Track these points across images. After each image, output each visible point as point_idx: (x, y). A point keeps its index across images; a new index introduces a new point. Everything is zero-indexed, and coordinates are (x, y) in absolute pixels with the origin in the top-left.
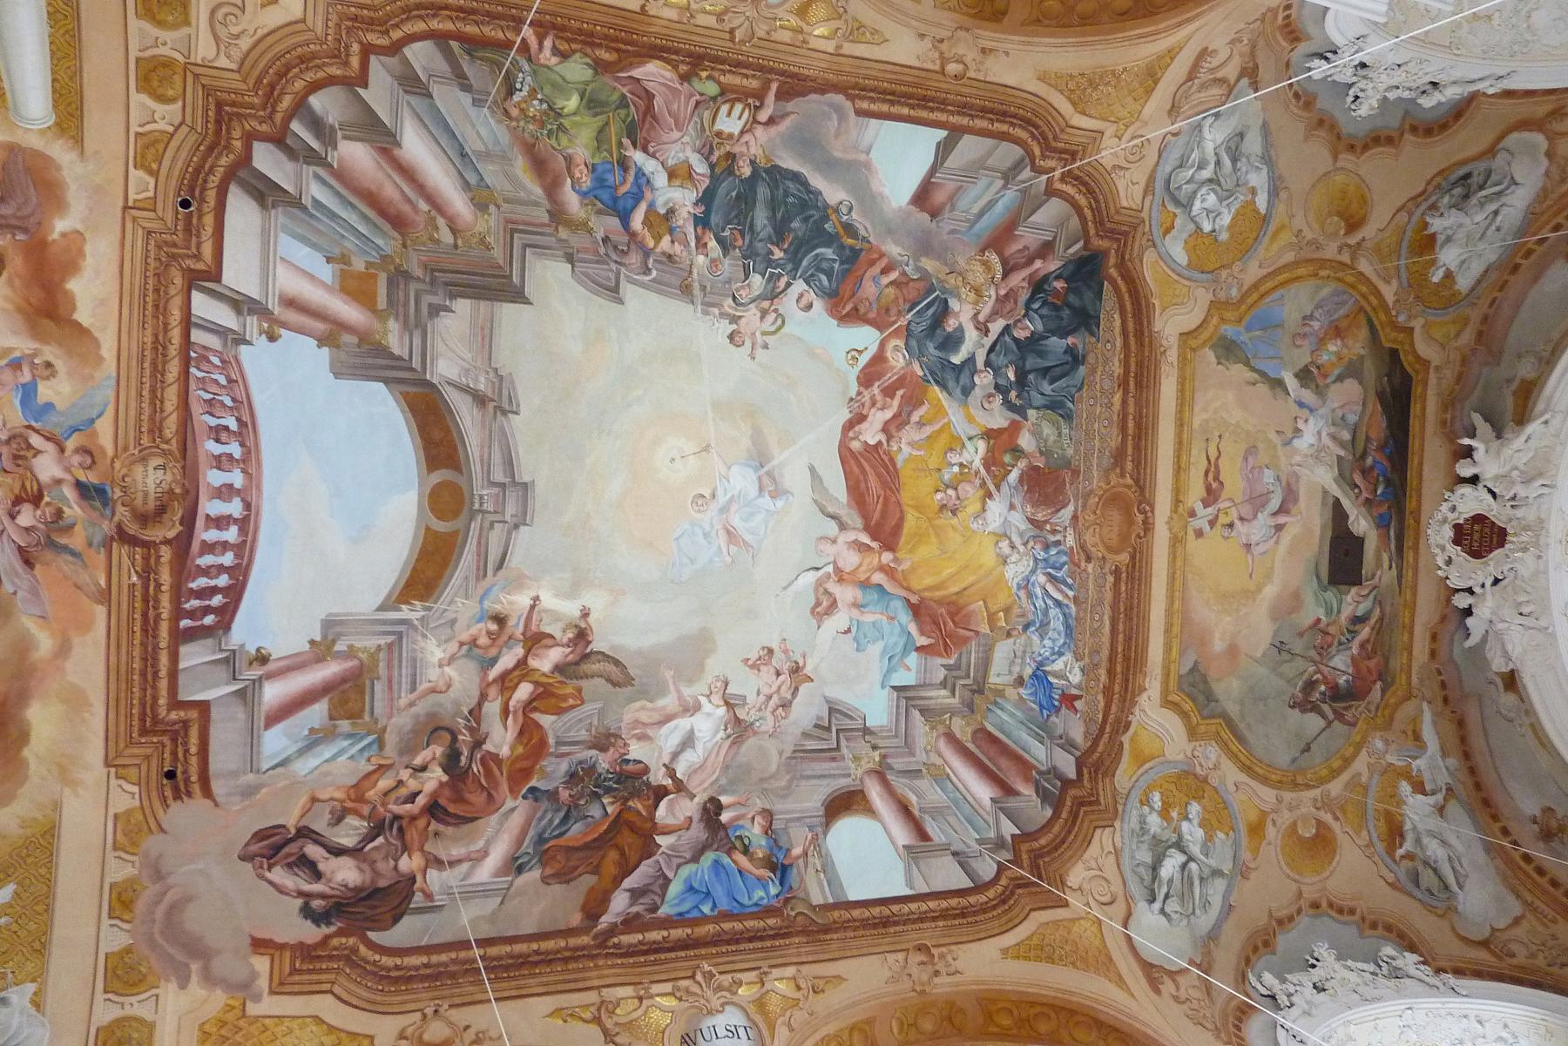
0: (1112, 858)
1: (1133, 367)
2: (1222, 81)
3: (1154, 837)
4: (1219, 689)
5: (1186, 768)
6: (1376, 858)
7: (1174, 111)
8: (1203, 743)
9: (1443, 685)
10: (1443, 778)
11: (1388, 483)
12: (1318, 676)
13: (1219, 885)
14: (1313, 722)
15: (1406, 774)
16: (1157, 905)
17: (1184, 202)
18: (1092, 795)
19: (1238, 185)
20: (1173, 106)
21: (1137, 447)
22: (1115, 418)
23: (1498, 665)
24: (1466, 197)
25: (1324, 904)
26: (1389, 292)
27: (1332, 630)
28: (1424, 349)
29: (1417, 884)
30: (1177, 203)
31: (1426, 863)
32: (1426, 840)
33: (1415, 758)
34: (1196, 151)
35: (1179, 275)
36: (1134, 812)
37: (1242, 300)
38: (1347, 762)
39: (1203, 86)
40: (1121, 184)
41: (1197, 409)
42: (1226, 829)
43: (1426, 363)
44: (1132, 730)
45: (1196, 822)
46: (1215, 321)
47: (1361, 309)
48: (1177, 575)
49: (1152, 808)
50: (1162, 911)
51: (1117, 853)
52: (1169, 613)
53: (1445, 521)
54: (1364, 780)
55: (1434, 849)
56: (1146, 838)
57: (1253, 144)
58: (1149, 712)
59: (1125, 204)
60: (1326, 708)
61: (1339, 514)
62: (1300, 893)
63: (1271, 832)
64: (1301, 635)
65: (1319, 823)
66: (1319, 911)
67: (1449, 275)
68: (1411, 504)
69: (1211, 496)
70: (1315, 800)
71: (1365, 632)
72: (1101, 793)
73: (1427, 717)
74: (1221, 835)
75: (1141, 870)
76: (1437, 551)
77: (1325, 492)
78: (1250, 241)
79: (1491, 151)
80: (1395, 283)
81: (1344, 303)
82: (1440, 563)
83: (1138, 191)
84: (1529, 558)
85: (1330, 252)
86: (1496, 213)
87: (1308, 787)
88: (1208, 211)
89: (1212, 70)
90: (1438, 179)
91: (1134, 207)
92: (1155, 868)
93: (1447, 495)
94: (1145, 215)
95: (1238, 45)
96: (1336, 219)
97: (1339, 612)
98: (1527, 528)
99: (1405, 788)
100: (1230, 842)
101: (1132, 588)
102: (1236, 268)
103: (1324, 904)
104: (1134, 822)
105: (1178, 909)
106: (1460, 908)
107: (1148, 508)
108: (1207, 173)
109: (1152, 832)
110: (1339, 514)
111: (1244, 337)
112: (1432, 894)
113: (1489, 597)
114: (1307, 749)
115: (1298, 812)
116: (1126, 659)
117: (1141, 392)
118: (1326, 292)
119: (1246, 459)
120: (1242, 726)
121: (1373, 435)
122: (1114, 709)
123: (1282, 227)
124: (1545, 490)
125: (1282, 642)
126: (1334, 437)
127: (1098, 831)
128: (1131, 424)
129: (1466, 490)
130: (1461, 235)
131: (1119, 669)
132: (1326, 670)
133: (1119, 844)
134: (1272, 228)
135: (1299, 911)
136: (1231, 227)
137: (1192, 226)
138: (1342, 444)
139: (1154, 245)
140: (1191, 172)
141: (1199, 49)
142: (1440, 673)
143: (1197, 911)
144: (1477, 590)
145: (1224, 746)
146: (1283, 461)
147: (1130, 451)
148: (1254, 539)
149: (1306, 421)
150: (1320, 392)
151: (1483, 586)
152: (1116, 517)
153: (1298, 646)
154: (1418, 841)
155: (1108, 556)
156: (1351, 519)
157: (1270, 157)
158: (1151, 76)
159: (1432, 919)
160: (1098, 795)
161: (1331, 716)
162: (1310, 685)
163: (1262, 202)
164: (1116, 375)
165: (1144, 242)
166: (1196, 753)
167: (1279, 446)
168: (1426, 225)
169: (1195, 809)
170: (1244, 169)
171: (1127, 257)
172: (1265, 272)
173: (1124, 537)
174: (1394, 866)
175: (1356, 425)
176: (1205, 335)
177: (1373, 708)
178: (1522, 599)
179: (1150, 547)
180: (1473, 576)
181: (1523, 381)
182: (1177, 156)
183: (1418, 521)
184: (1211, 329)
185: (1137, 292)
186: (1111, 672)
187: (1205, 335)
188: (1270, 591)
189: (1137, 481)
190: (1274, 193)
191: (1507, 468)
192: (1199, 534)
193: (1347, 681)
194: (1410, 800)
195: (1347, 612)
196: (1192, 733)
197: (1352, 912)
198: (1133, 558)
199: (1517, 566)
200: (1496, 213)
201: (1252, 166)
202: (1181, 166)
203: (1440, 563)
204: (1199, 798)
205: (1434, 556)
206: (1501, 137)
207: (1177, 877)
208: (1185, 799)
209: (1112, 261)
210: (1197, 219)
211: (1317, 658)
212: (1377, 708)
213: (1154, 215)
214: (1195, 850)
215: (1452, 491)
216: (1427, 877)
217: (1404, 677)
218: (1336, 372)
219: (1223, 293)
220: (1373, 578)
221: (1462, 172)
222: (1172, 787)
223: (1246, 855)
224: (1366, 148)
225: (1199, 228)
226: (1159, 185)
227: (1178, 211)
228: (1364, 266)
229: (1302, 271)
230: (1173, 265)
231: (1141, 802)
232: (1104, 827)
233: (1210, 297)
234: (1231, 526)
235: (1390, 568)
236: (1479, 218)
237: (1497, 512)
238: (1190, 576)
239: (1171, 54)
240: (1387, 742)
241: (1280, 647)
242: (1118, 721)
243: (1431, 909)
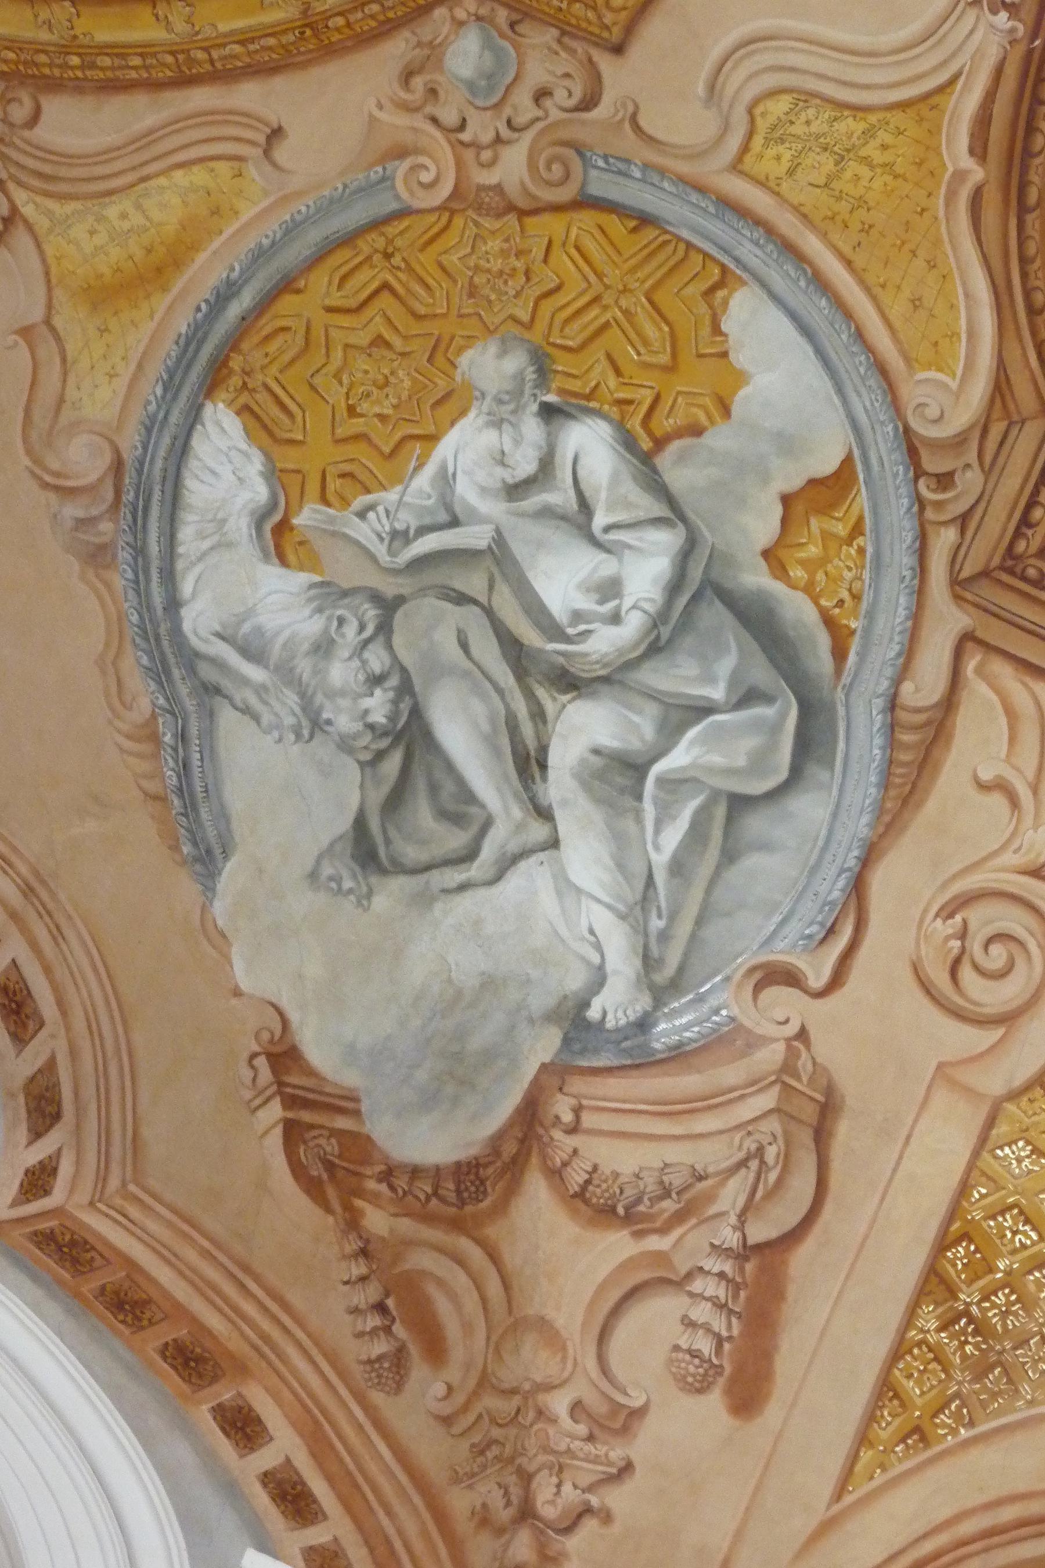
20: (822, 1136)
34: (661, 859)
35: (791, 250)
141: (773, 1413)
157: (160, 674)
165: (970, 481)
182: (751, 861)
201: (286, 673)
210: (649, 506)
219: (537, 74)
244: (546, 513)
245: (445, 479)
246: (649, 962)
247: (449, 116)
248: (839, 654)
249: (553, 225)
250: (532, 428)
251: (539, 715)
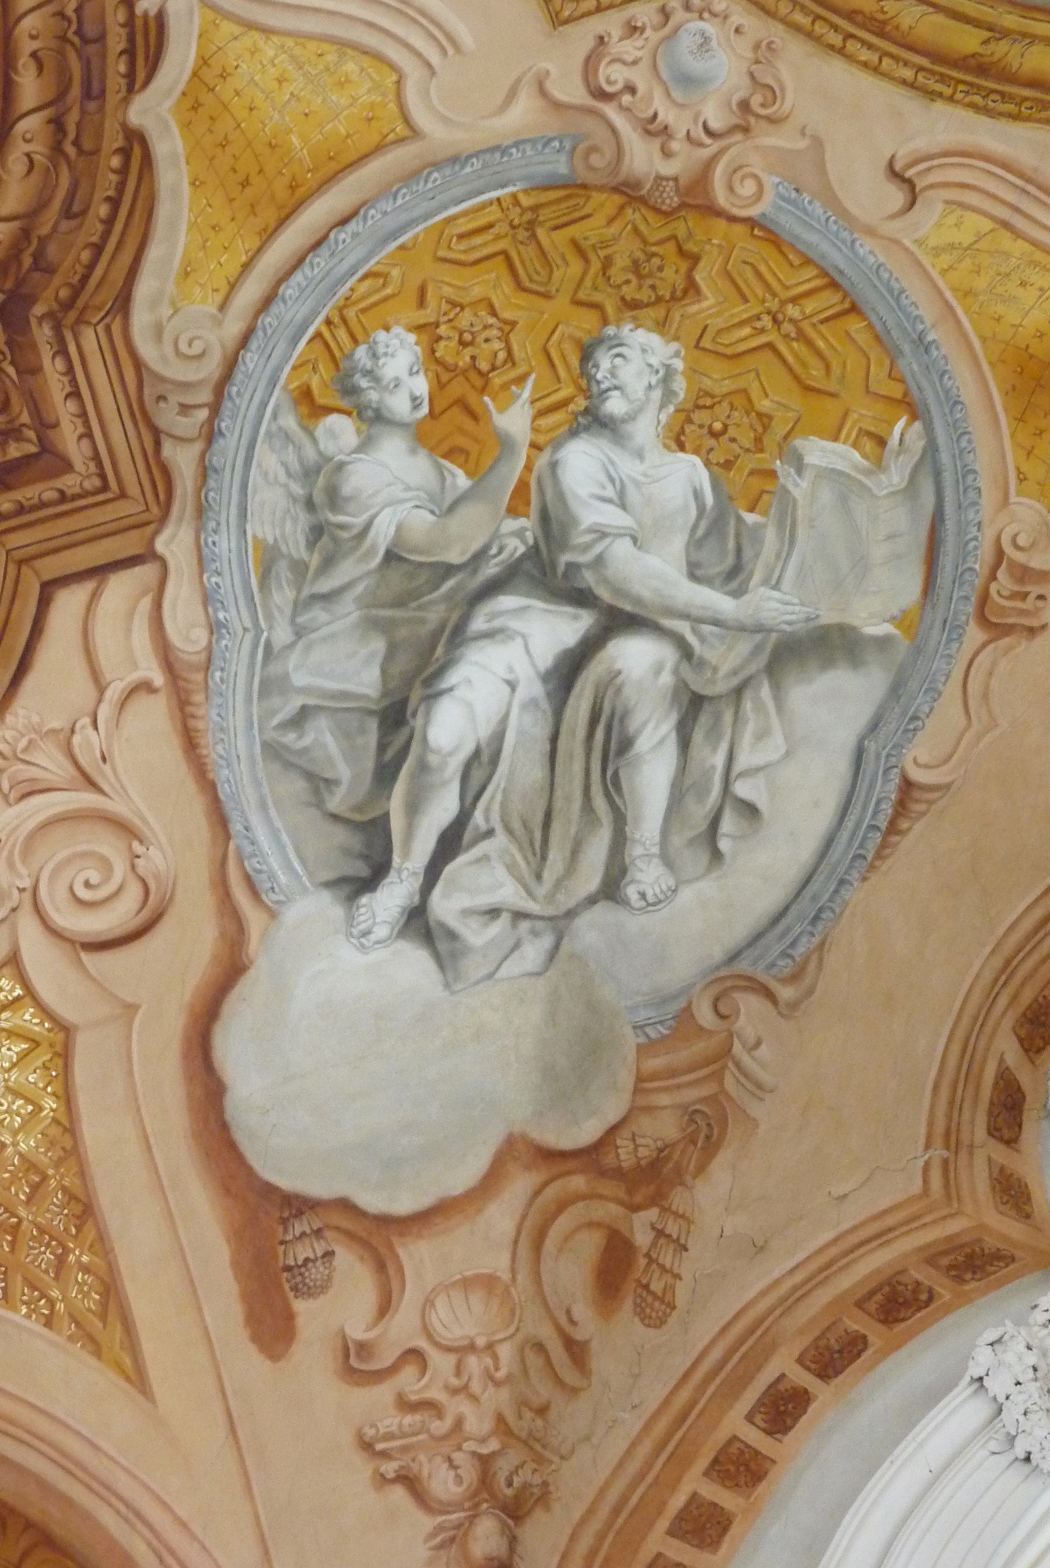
3: (391, 557)
5: (562, 168)
56: (346, 570)
72: (64, 411)
100: (896, 476)
109: (383, 533)
160: (45, 425)
208: (585, 323)
231: (305, 395)
232: (100, 572)
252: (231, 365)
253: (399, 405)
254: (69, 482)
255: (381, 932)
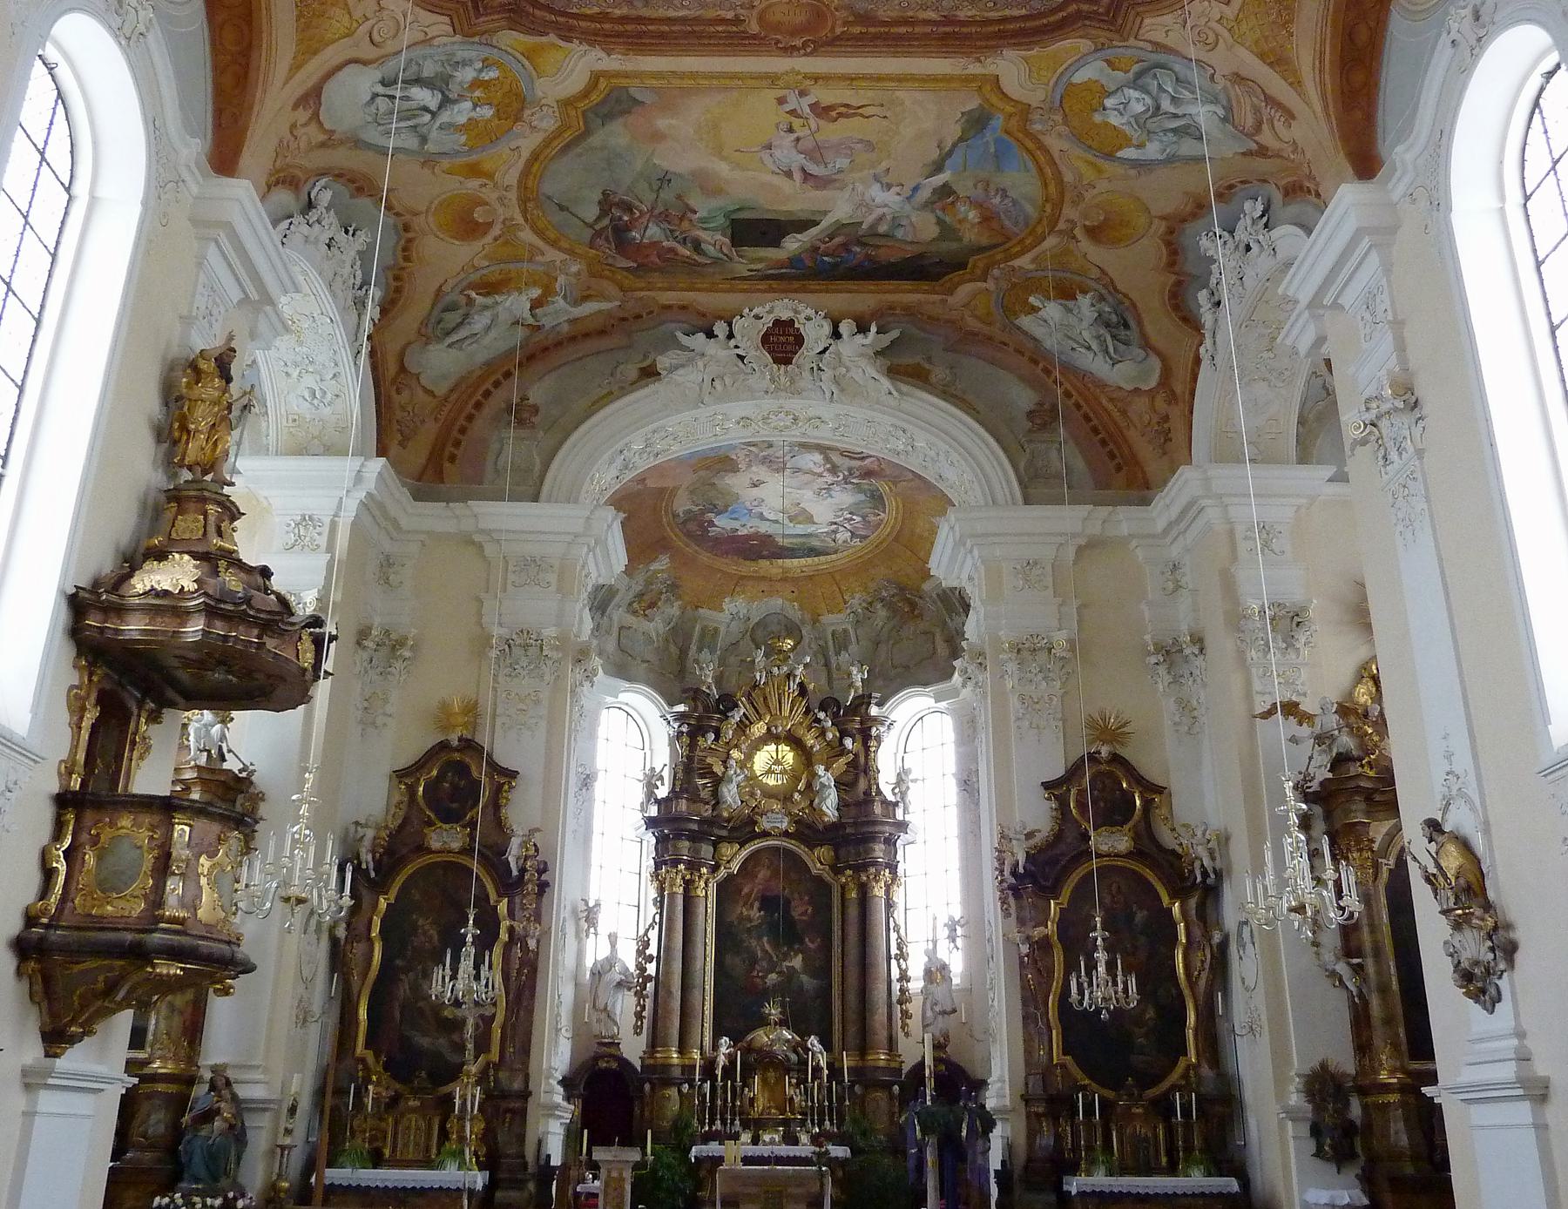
0: (421, 36)
1: (964, 30)
2: (1258, 127)
3: (451, 76)
4: (617, 126)
6: (462, 275)
7: (1238, 78)
8: (557, 114)
9: (639, 317)
10: (547, 322)
11: (836, 265)
12: (638, 214)
13: (412, 142)
14: (591, 212)
15: (548, 291)
16: (380, 89)
17: (1140, 82)
18: (485, 8)
19: (1149, 132)
21: (876, 37)
22: (910, 14)
23: (663, 362)
24: (1107, 325)
25: (410, 235)
26: (1024, 262)
27: (685, 224)
28: (965, 290)
29: (444, 310)
30: (1139, 75)
31: (466, 316)
32: (488, 314)
33: (565, 297)
36: (474, 53)
37: (1028, 134)
38: (554, 244)
39: (1256, 110)
40: (1168, 19)
41: (918, 95)
42: (470, 143)
43: (951, 292)
44: (562, 43)
45: (473, 114)
46: (1009, 109)
47: (1009, 239)
48: (736, 81)
49: (481, 71)
50: (375, 96)
51: (427, 41)
52: (693, 75)
53: (796, 312)
54: (539, 258)
55: (480, 322)
56: (448, 68)
57: (1187, 147)
58: (584, 59)
59: (1147, 21)
60: (606, 222)
61: (802, 225)
62: (416, 214)
63: (473, 184)
64: (679, 197)
65: (490, 225)
66: (402, 233)
67: (1035, 310)
68: (813, 285)
69: (821, 111)
70: (512, 219)
71: (685, 251)
72: (489, 18)
73: (605, 306)
74: (463, 139)
75: (415, 68)
76: (767, 307)
77: (825, 213)
78: (1089, 142)
79: (1147, 345)
80: (1032, 267)
81: (1016, 223)
82: (756, 311)
83: (1159, 36)
84: (766, 383)
85: (1069, 212)
86: (1089, 348)
87: (524, 212)
88: (1126, 105)
89: (1271, 121)
90: (1127, 303)
91: (1141, 32)
92: (418, 81)
93: (823, 314)
94: (1132, 41)
95: (1290, 149)
96: (1102, 218)
97: (705, 229)
98: (792, 381)
99: (536, 293)
100: (458, 148)
101: (720, 38)
102: (1062, 129)
103: (410, 235)
104: (461, 54)
105: (381, 111)
106: (431, 347)
107: (809, 50)
108: (1166, 105)
109: (456, 74)
110: (802, 225)
111: (989, 136)
112: (439, 323)
113: (725, 353)
114: (562, 208)
115: (497, 206)
116: (640, 35)
117: (939, 39)
118: (1029, 209)
119: (861, 141)
120: (579, 150)
121: (882, 251)
122: (583, 24)
123: (1100, 171)
124: (828, 395)
125: (670, 181)
126: (881, 218)
127: (447, 19)
128: (903, 30)
129: (827, 328)
130: (1072, 320)
131: (629, 28)
132: (644, 220)
133: (436, 41)
134: (1102, 163)
135: (397, 214)
136: (1107, 124)
137: (1113, 88)
138: (873, 226)
139: (1096, 50)
140: (1170, 90)
142: (648, 314)
143: (380, 128)
144: (732, 343)
145: (558, 134)
146: (856, 175)
147: (872, 30)
148: (777, 153)
149: (899, 194)
150: (928, 205)
151: (736, 347)
152: (800, 18)
153: (667, 195)
154: (486, 307)
155: (755, 12)
156: (798, 236)
157: (1172, 163)
158: (1279, 61)
159: (416, 326)
160: (486, 15)
161: (597, 227)
162: (629, 208)
163: (1129, 153)
164: (958, 13)
165: (1101, 40)
166: (545, 108)
167: (872, 171)
168: (1085, 292)
169: (486, 112)
170: (1165, 139)
171: (1088, 23)
172: (1056, 155)
173: (777, 28)
174: (458, 290)
175: (893, 237)
176: (994, 100)
177: (610, 261)
178: (728, 380)
179: (769, 53)
180: (745, 339)
181: (929, 372)
183: (796, 291)
184: (1000, 105)
185: (1044, 33)
186: (624, 20)
187: (994, 100)
188: (723, 169)
189: (838, 38)
190: (1136, 164)
191: (848, 364)
192: (781, 101)
193: (634, 239)
194: (524, 298)
195: (704, 235)
196: (567, 104)
197: (407, 259)
198: (754, 37)
199: (758, 374)
200: (1089, 348)
201: (1167, 146)
202: (1177, 79)
203: (756, 311)
204: (498, 115)
205: (762, 305)
206: (1159, 354)
207: (413, 104)
209: (1085, 7)
211: (656, 212)
212: (611, 265)
213: (1129, 51)
214: (445, 117)
215: (825, 317)
216: (452, 318)
217: (643, 285)
218: (947, 219)
220: (741, 257)
221: (1132, 323)
222: (506, 88)
223: (446, 163)
224: (1168, 244)
225: (1109, 94)
226: (1161, 58)
227: (1131, 75)
228: (1051, 241)
229: (1052, 189)
230: (1073, 68)
231: (487, 59)
232: (453, 27)
233: (1034, 105)
234: (791, 130)
235: (752, 271)
236: (1086, 334)
237: (806, 355)
238: (735, 94)
239: (1297, 84)
240: (578, 273)
241: (665, 179)
242: (571, 29)
243: (425, 323)
244: (1125, 108)
245: (1123, 124)
246: (1212, 102)
247: (1050, 128)
248: (1144, 61)
249: (1067, 110)
250: (1107, 112)
251: (1165, 113)
252: (495, 47)
253: (483, 74)
254: (473, 18)
255: (373, 90)
